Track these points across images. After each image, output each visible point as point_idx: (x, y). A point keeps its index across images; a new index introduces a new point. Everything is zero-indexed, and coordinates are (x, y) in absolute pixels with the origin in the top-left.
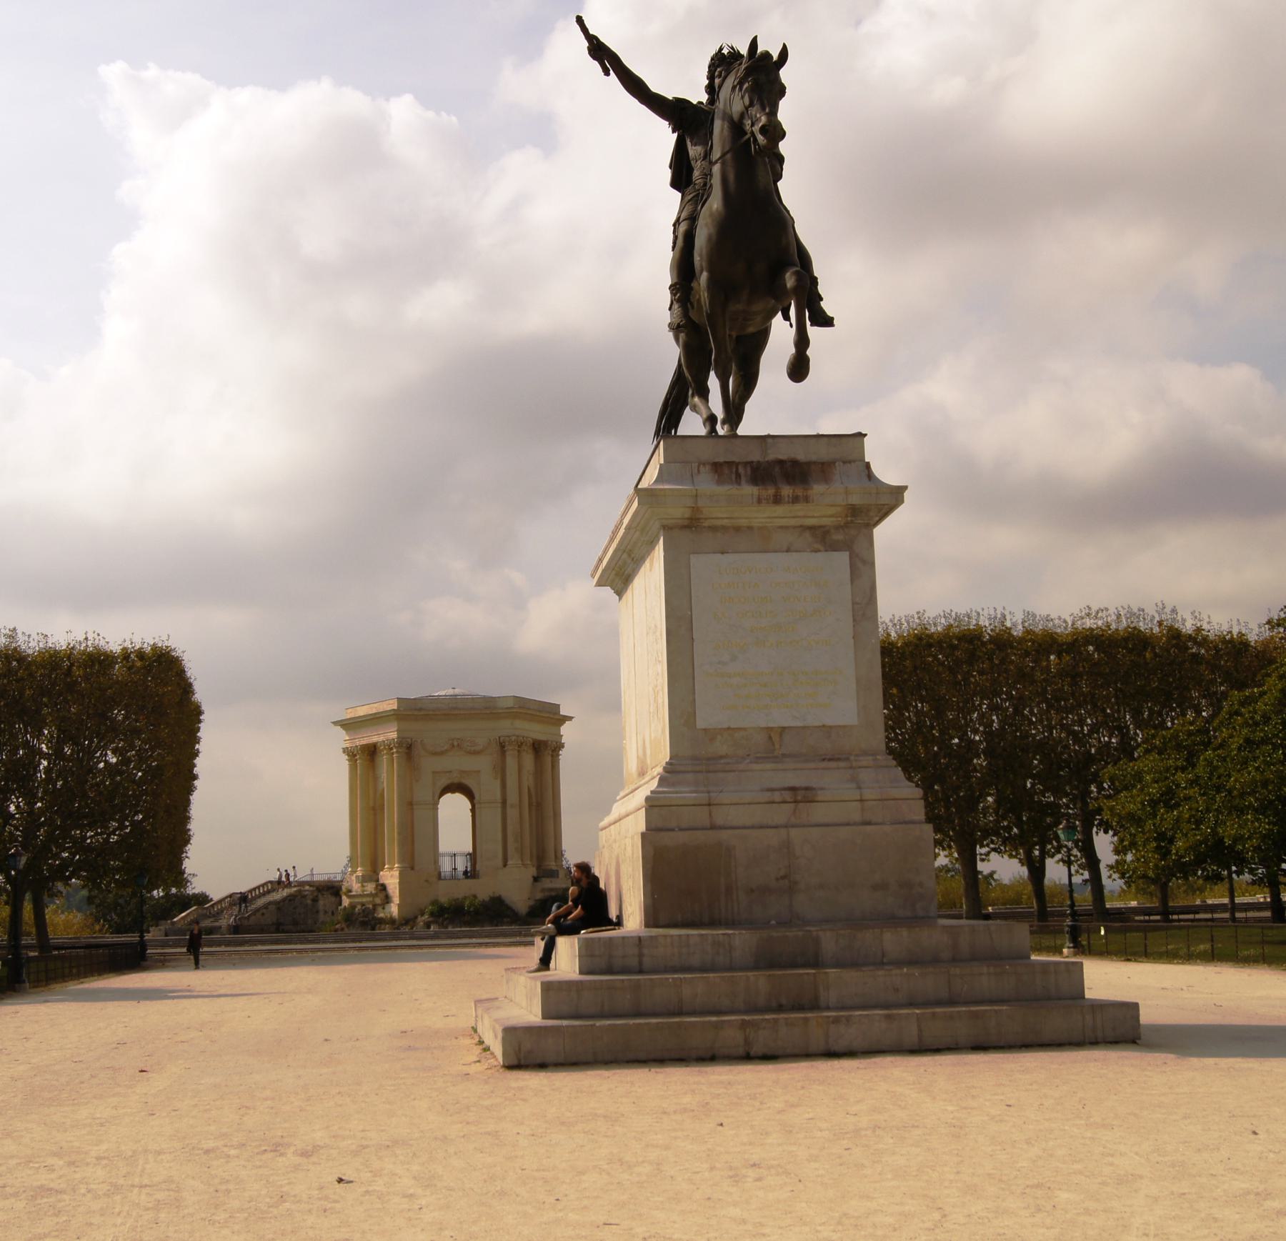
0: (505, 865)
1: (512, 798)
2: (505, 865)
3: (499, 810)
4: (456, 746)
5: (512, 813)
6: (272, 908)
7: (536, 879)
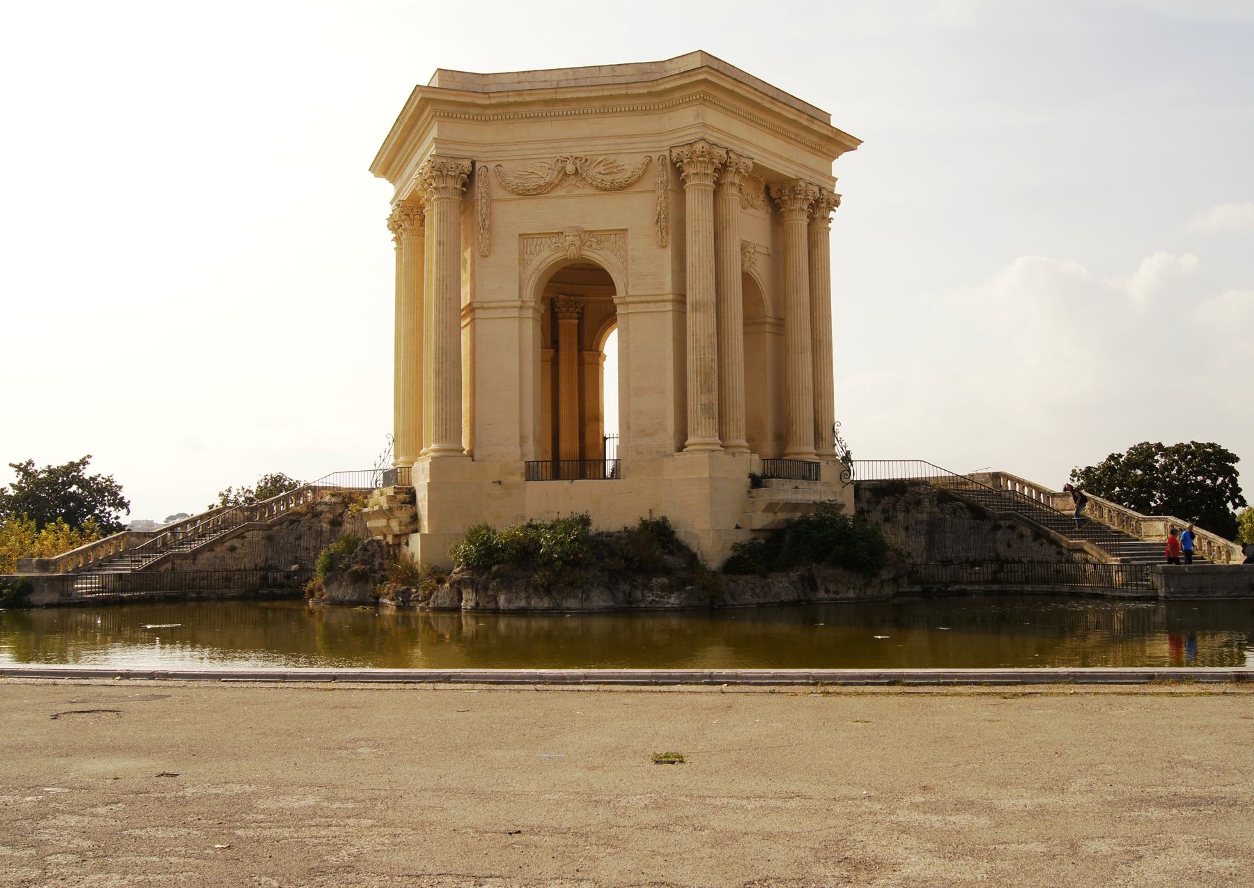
0: (681, 448)
1: (700, 287)
2: (681, 448)
3: (669, 319)
4: (572, 173)
5: (700, 324)
6: (255, 536)
7: (757, 482)
